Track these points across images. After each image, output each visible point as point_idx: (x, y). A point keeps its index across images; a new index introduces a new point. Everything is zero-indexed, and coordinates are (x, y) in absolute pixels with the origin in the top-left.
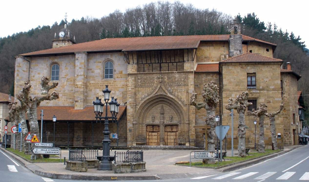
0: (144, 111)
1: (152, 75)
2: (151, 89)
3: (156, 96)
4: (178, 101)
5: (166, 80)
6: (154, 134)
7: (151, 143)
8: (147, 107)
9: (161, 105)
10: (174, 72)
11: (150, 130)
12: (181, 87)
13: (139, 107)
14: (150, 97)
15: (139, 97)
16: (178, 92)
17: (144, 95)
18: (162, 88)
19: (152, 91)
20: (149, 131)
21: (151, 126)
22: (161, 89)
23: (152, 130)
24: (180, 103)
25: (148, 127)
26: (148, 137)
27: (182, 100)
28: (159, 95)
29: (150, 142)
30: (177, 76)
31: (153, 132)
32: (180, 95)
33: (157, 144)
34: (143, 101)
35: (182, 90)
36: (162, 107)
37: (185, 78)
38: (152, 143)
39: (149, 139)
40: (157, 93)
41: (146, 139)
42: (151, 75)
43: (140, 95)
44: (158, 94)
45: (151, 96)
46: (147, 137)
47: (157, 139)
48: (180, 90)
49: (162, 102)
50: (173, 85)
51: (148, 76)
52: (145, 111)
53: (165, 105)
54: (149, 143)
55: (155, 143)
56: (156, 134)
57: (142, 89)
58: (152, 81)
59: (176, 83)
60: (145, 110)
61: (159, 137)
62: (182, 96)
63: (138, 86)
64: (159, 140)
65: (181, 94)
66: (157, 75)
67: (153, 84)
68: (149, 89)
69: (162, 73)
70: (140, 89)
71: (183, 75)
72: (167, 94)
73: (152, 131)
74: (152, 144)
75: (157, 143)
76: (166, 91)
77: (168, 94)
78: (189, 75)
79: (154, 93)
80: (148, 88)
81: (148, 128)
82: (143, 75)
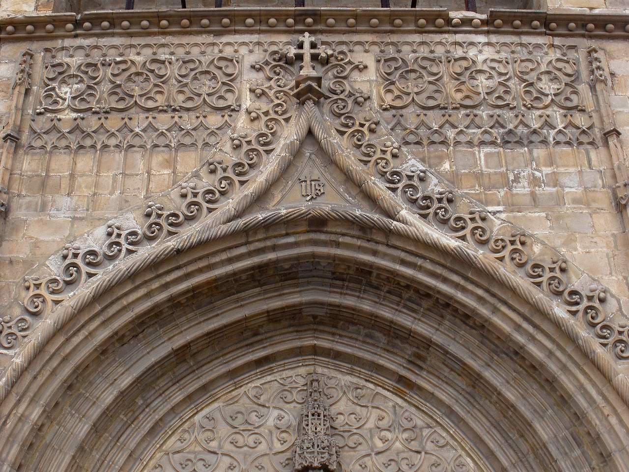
0: (83, 429)
1: (210, 39)
2: (188, 162)
3: (247, 232)
4: (540, 296)
5: (368, 82)
8: (126, 381)
9: (296, 374)
10: (449, 21)
12: (540, 152)
13: (19, 361)
14: (172, 243)
15: (36, 245)
16: (512, 206)
17: (100, 231)
18: (330, 160)
19: (207, 182)
22: (311, 168)
24: (560, 311)
27: (577, 282)
28: (288, 223)
30: (483, 50)
32: (539, 232)
34: (85, 290)
35: (554, 180)
36: (314, 390)
37: (574, 79)
40: (260, 198)
42: (199, 39)
43: (58, 228)
44: (283, 212)
45: (190, 233)
48: (535, 181)
49: (309, 342)
50: (451, 134)
51: (175, 50)
52: (97, 429)
53: (346, 379)
57: (85, 162)
58: (206, 86)
59: (484, 113)
60: (95, 413)
62: (569, 242)
63: (52, 139)
65: (556, 219)
66: (265, 38)
67: (214, 120)
68: (171, 164)
69: (317, 16)
70: (61, 164)
71: (546, 52)
72: (390, 215)
76: (379, 187)
77: (404, 212)
78: (610, 56)
79: (230, 205)
80: (158, 158)
82: (117, 41)
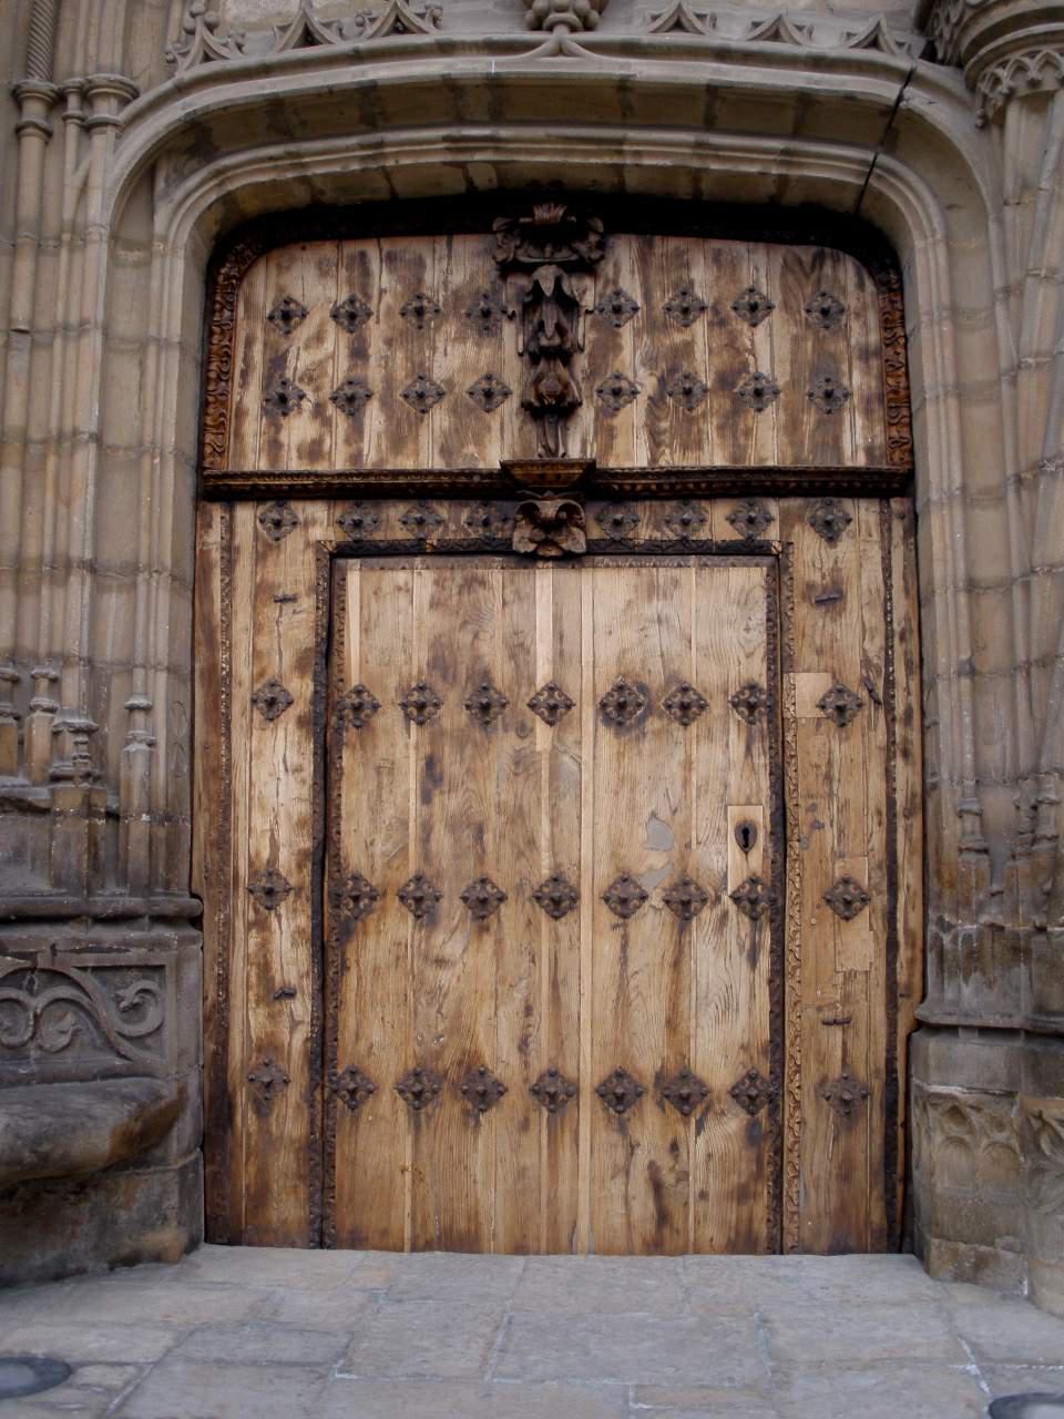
6: (587, 617)
7: (456, 1087)
11: (372, 445)
20: (358, 490)
21: (457, 267)
23: (498, 444)
25: (311, 281)
26: (272, 774)
29: (380, 1039)
31: (550, 509)
33: (770, 1149)
38: (481, 1093)
39: (335, 900)
41: (171, 885)
46: (208, 782)
47: (765, 904)
54: (333, 1082)
55: (683, 1095)
56: (703, 619)
61: (851, 779)
64: (860, 944)
73: (503, 488)
74: (492, 1160)
75: (762, 1095)
81: (318, 353)
